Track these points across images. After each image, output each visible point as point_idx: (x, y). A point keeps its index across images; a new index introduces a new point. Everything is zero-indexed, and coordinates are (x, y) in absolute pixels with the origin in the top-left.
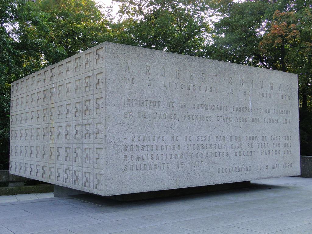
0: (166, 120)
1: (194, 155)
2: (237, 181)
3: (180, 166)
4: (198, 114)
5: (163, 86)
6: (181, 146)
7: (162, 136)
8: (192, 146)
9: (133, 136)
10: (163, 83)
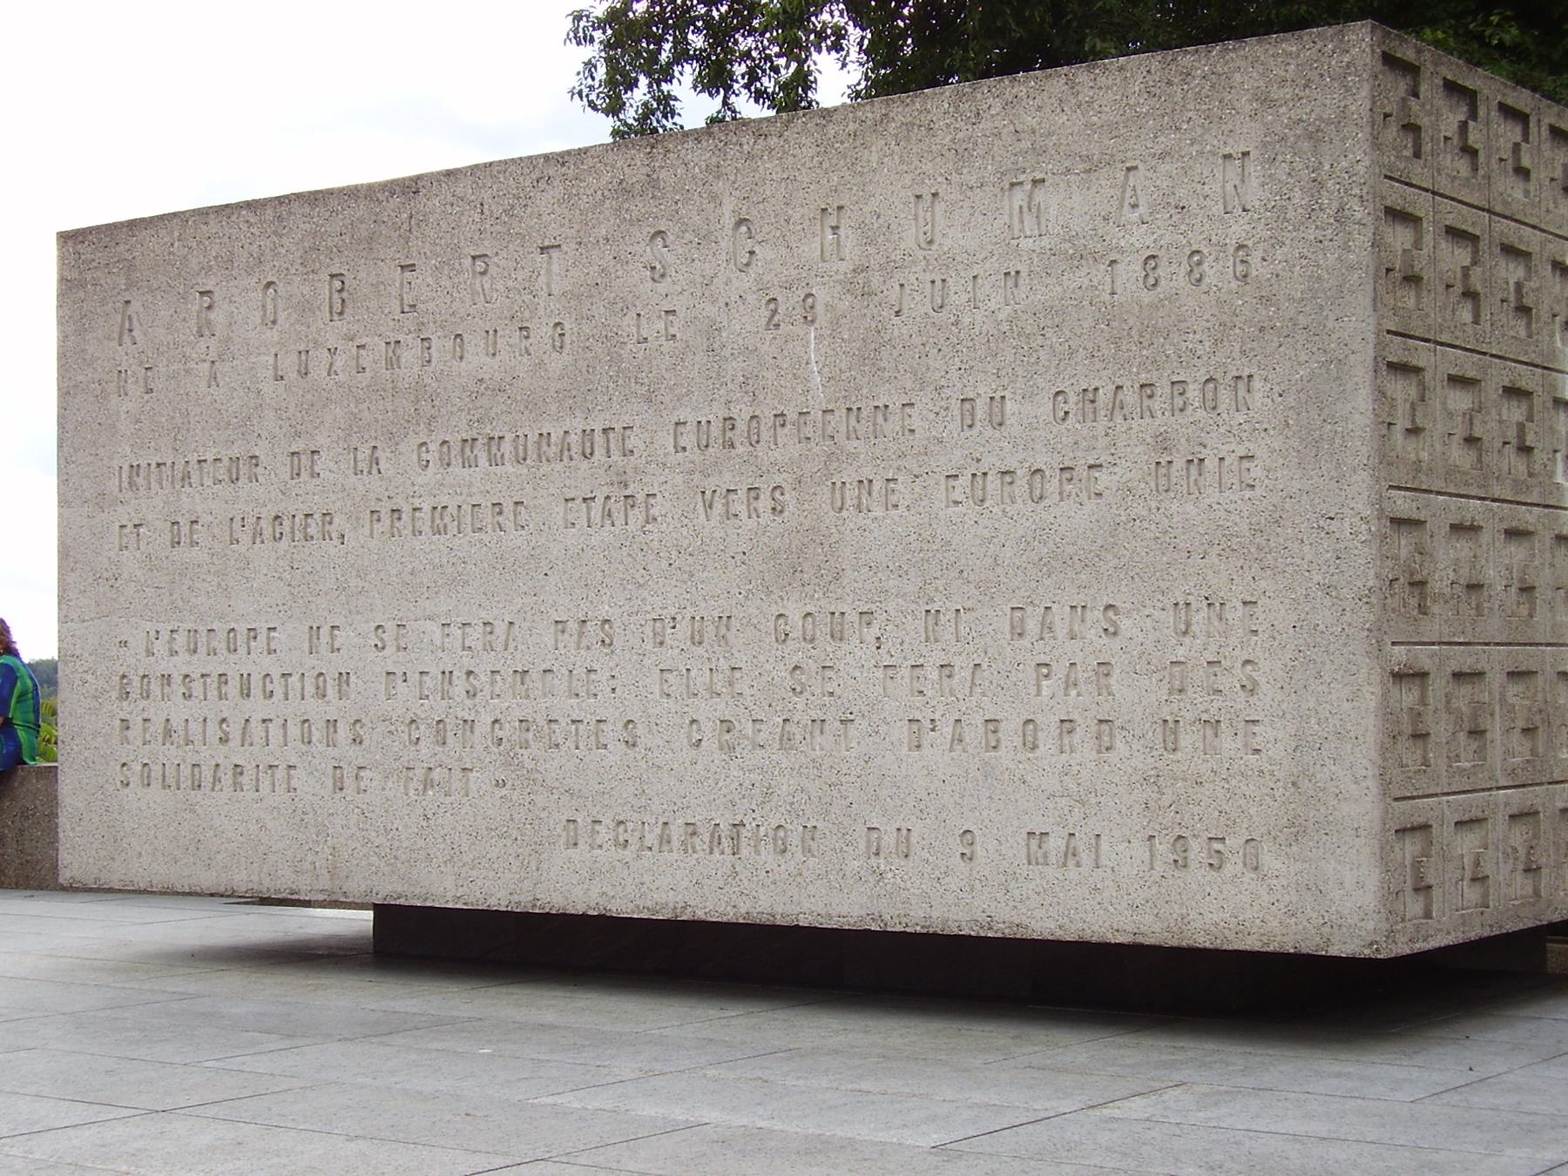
0: (284, 544)
1: (422, 727)
2: (701, 915)
3: (349, 783)
4: (444, 500)
5: (271, 373)
6: (353, 678)
7: (265, 631)
8: (414, 678)
9: (152, 634)
10: (271, 360)
